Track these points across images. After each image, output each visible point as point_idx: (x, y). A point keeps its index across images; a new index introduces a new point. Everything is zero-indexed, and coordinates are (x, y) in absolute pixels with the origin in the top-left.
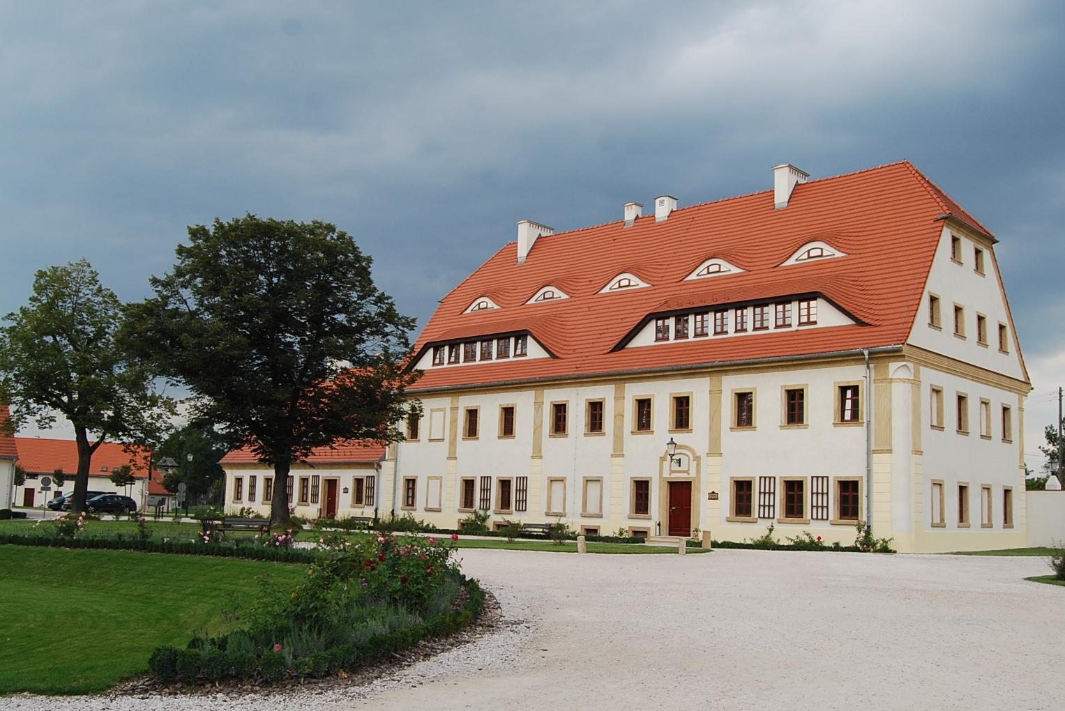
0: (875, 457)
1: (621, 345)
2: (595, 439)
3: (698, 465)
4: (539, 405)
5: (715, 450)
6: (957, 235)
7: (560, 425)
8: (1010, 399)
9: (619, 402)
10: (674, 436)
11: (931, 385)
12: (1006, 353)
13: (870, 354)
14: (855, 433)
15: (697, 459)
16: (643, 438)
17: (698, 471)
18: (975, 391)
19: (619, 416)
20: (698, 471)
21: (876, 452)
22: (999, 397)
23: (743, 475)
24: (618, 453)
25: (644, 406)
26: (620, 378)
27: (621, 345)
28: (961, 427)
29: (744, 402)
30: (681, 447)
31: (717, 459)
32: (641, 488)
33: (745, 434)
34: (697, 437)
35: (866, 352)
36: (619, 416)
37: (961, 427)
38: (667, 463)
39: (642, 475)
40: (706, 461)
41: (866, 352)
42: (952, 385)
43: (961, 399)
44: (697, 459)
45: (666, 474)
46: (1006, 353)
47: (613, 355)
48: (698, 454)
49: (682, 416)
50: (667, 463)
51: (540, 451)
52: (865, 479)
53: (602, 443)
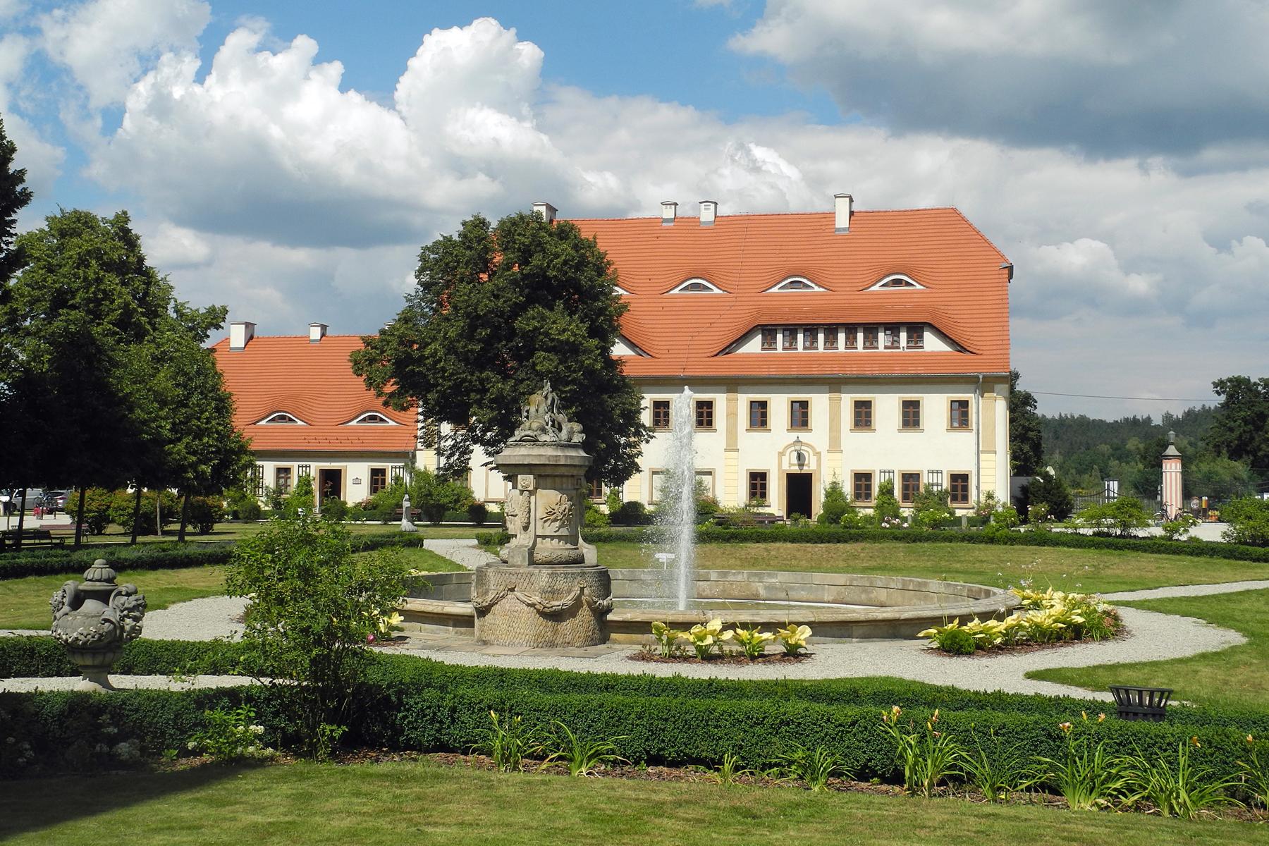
1: (728, 349)
3: (819, 460)
5: (835, 447)
14: (965, 440)
15: (818, 454)
17: (819, 464)
19: (732, 415)
20: (819, 464)
21: (984, 452)
23: (863, 468)
24: (732, 447)
27: (728, 349)
31: (838, 455)
33: (863, 436)
34: (817, 435)
36: (732, 415)
39: (758, 467)
40: (825, 457)
47: (720, 358)
49: (800, 415)
50: (785, 459)
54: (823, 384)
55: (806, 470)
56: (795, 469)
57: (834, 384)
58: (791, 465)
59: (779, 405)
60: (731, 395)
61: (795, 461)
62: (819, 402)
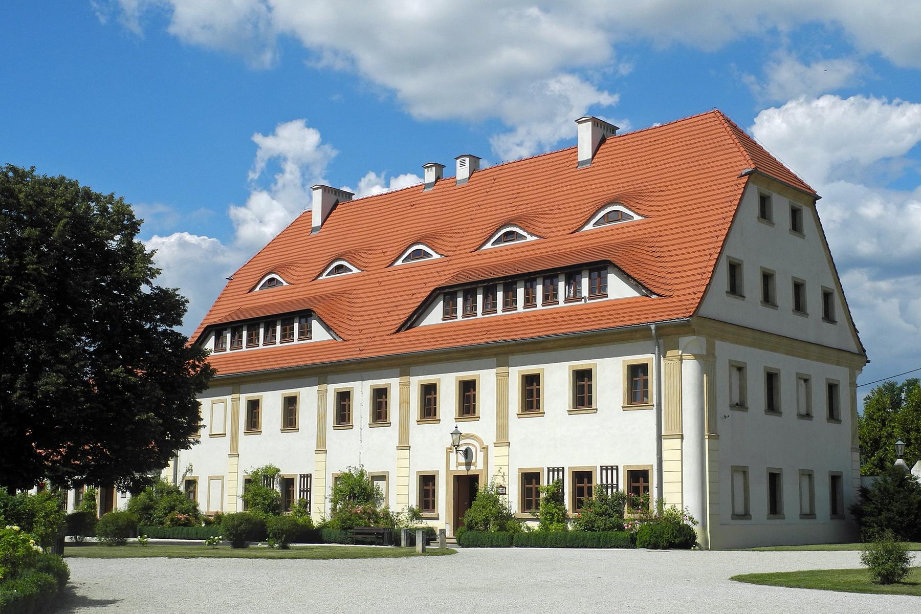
0: (666, 443)
2: (380, 432)
4: (322, 396)
6: (766, 192)
7: (343, 416)
8: (839, 373)
9: (403, 391)
10: (459, 424)
11: (730, 361)
12: (833, 321)
13: (657, 328)
14: (645, 418)
16: (429, 428)
17: (486, 463)
18: (790, 368)
19: (404, 403)
20: (486, 463)
22: (822, 372)
23: (531, 465)
24: (404, 445)
25: (429, 392)
26: (404, 364)
28: (772, 406)
29: (531, 384)
30: (468, 436)
31: (504, 450)
32: (427, 482)
35: (653, 327)
36: (404, 403)
37: (772, 406)
38: (453, 456)
40: (493, 451)
41: (653, 327)
42: (758, 361)
43: (771, 378)
44: (485, 449)
45: (453, 467)
46: (833, 321)
48: (485, 444)
51: (325, 445)
52: (655, 467)
53: (388, 435)
54: (489, 356)
55: (473, 470)
56: (462, 470)
57: (499, 353)
58: (459, 464)
59: (448, 386)
60: (405, 379)
61: (462, 459)
62: (487, 379)
